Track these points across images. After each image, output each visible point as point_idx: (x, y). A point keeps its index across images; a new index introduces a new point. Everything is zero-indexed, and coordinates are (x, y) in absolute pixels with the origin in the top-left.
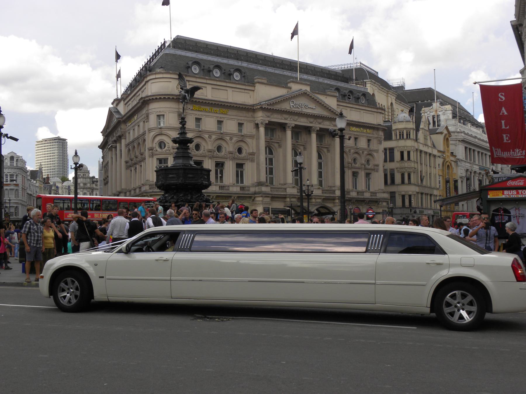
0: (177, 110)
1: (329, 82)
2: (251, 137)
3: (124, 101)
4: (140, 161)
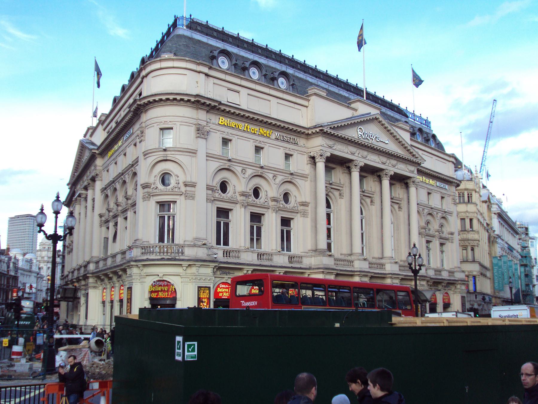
0: (194, 122)
1: (392, 115)
2: (304, 177)
3: (102, 125)
4: (125, 211)
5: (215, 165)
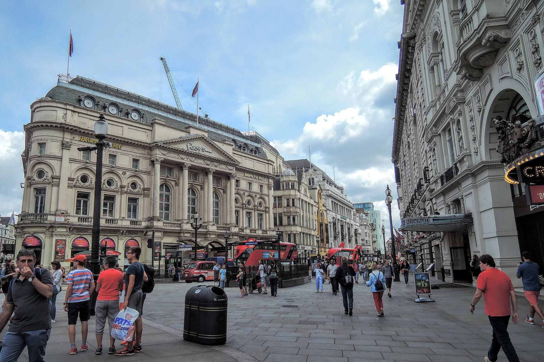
0: (61, 139)
5: (76, 166)
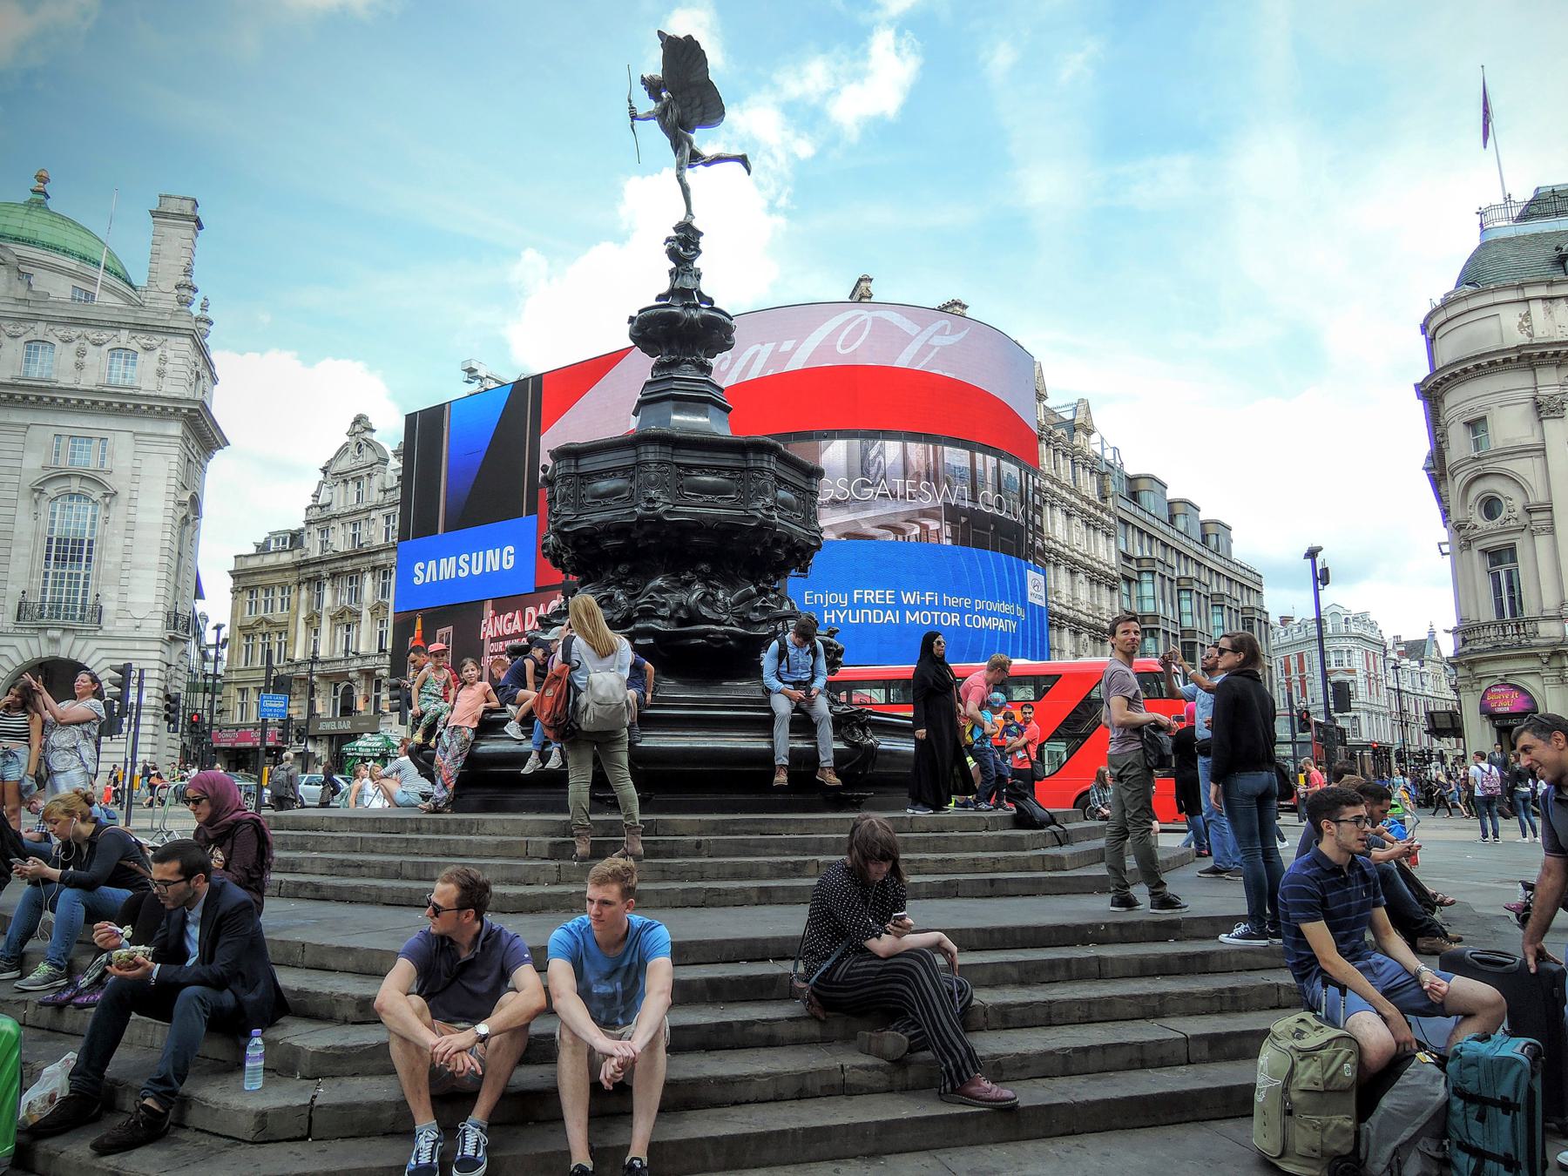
0: (1530, 393)
